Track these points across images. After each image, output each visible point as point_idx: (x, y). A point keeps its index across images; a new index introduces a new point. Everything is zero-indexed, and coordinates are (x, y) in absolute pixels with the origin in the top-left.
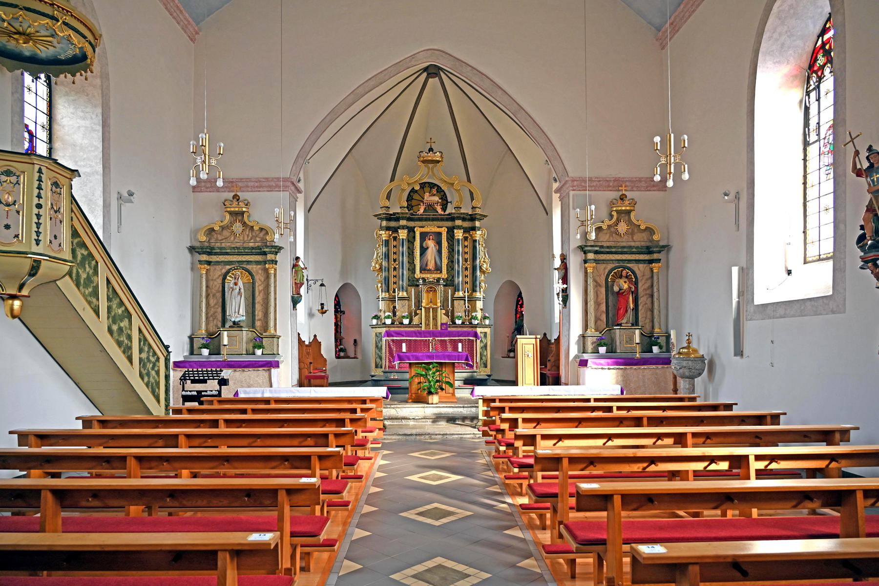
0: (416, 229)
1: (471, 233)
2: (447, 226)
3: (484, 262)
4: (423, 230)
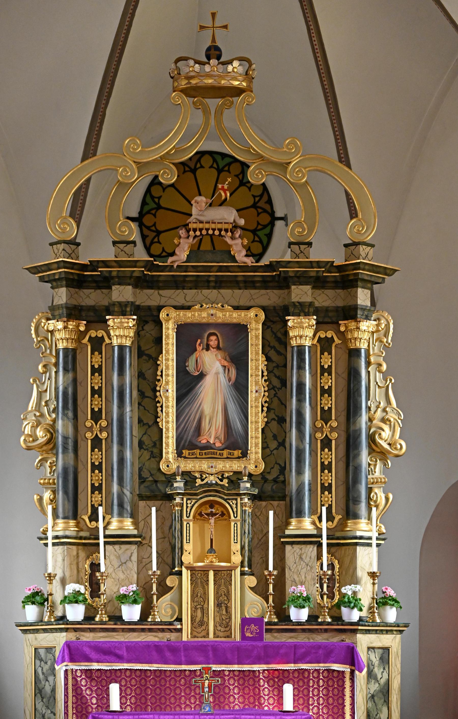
0: (163, 315)
1: (342, 329)
2: (266, 303)
3: (383, 420)
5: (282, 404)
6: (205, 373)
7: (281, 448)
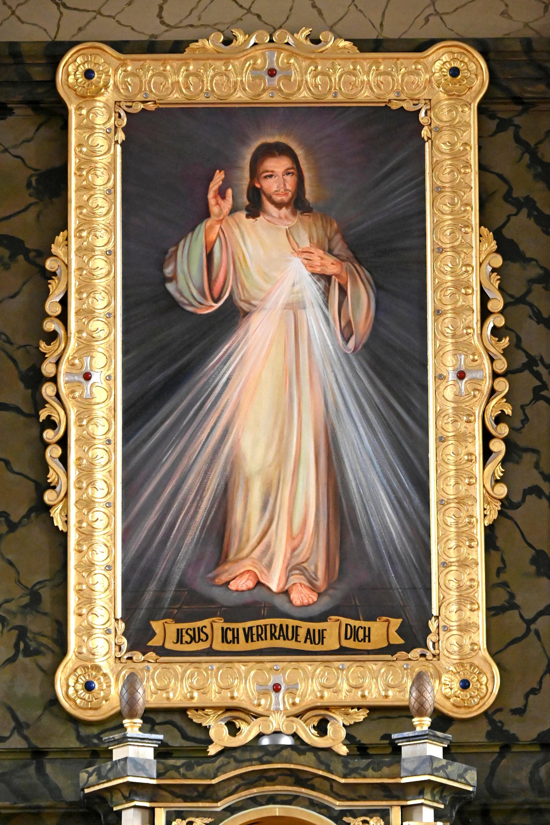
6: (244, 306)
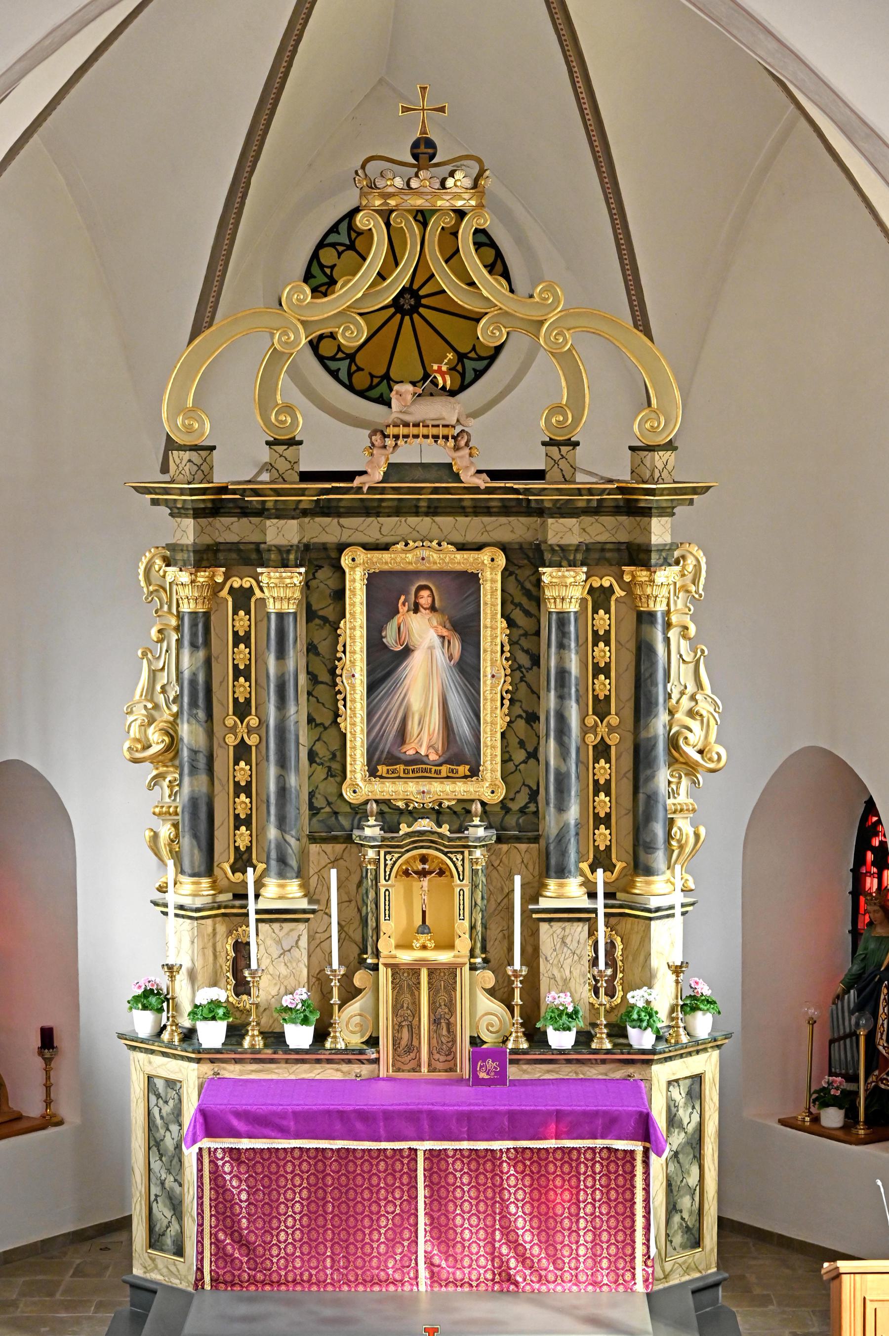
3: (691, 713)
4: (384, 560)
5: (533, 692)
7: (532, 761)
